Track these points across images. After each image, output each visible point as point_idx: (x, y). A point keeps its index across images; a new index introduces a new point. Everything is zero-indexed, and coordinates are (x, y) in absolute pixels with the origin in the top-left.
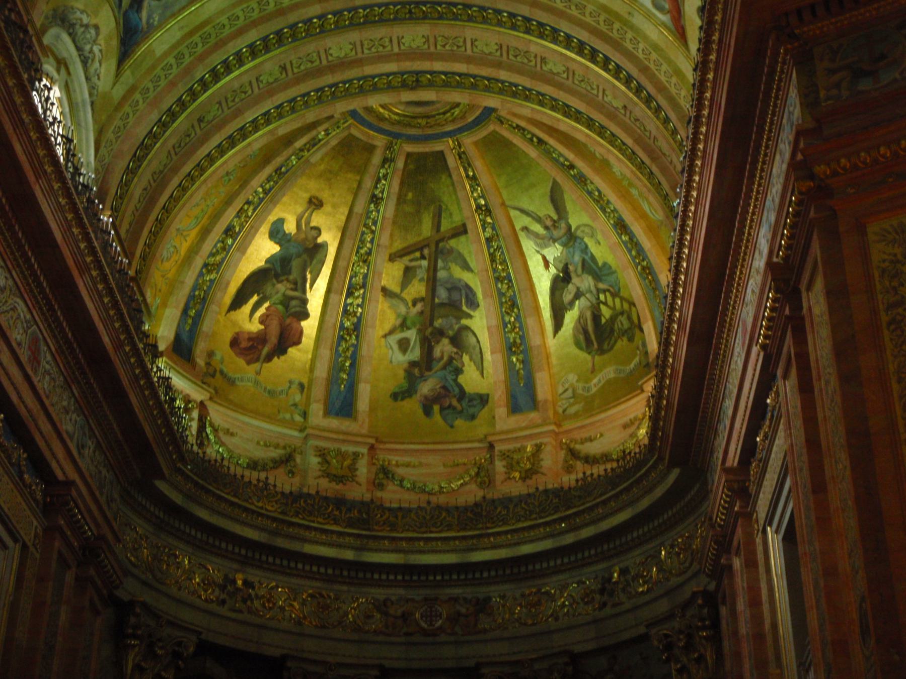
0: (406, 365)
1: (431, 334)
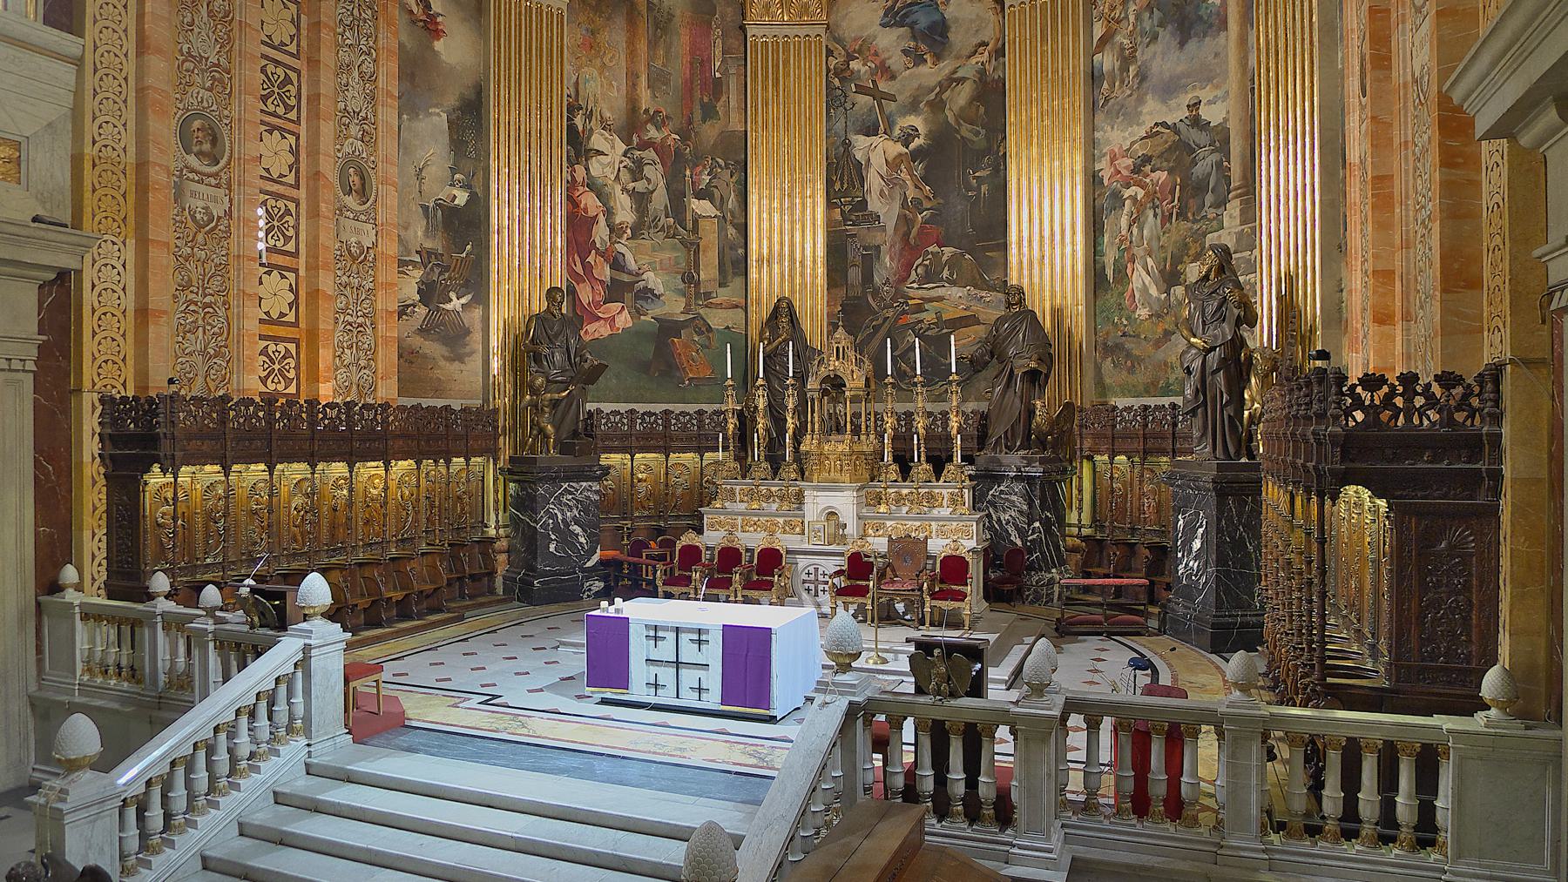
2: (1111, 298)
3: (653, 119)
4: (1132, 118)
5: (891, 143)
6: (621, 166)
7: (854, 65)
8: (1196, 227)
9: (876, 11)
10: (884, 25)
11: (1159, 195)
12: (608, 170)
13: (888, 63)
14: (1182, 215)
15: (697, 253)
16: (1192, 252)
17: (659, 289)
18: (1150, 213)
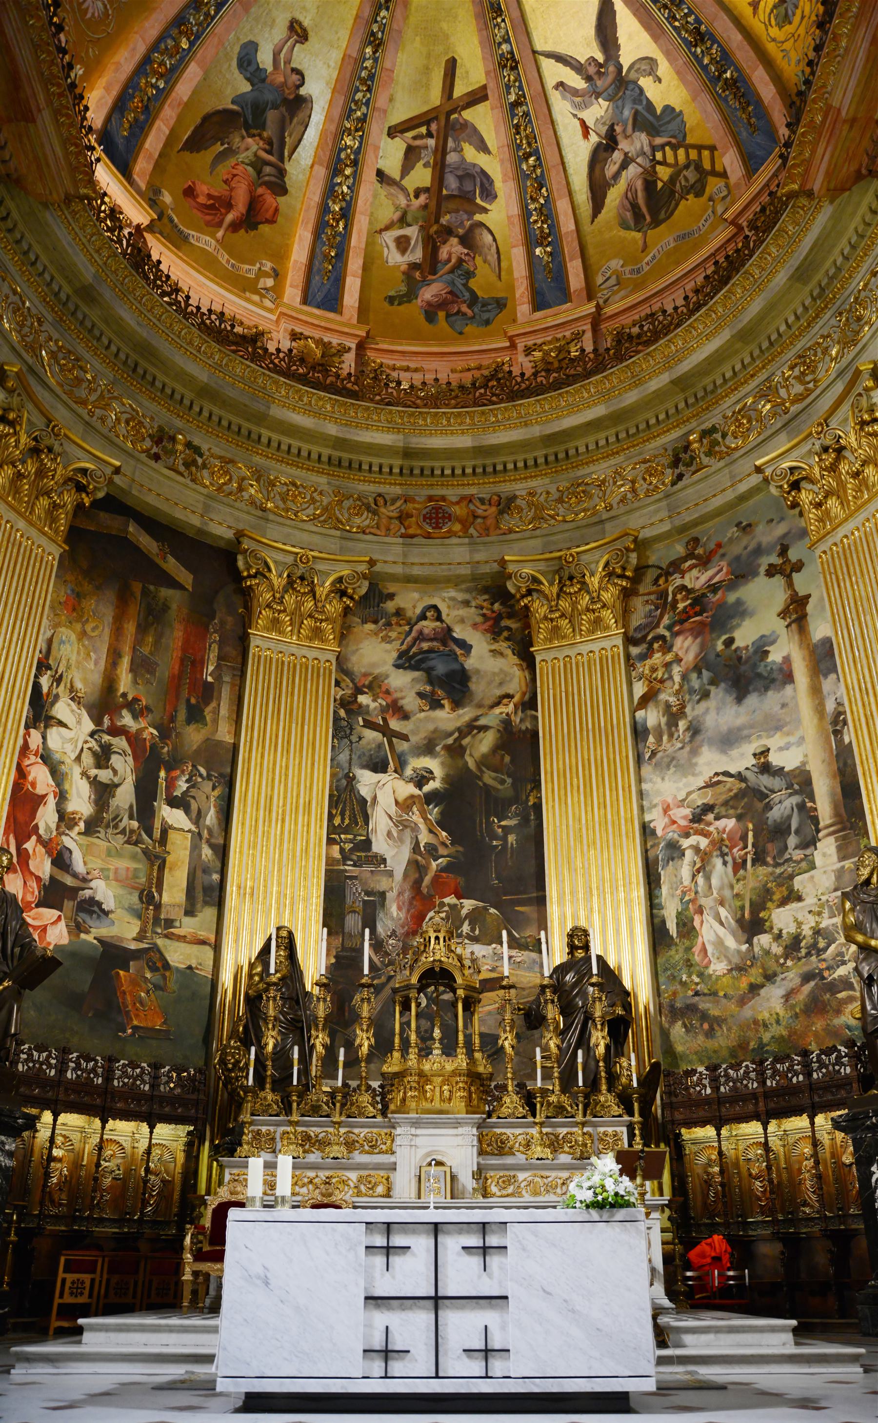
0: (404, 267)
1: (436, 232)
2: (676, 955)
3: (131, 705)
4: (687, 768)
5: (401, 783)
6: (86, 746)
7: (363, 699)
8: (778, 871)
9: (387, 651)
10: (397, 666)
11: (727, 843)
12: (69, 747)
13: (401, 702)
14: (759, 859)
15: (162, 868)
16: (776, 897)
17: (109, 904)
18: (718, 862)
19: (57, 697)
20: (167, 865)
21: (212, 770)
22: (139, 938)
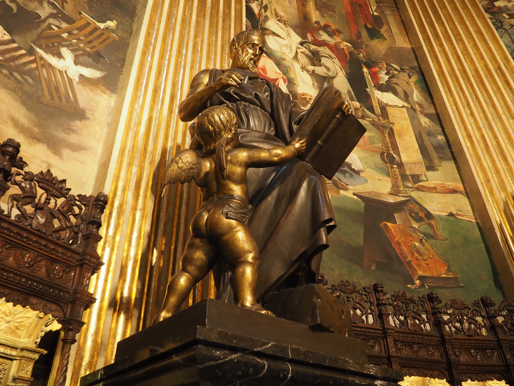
12: (286, 50)
19: (266, 18)
20: (395, 133)
21: (403, 65)
22: (395, 192)
